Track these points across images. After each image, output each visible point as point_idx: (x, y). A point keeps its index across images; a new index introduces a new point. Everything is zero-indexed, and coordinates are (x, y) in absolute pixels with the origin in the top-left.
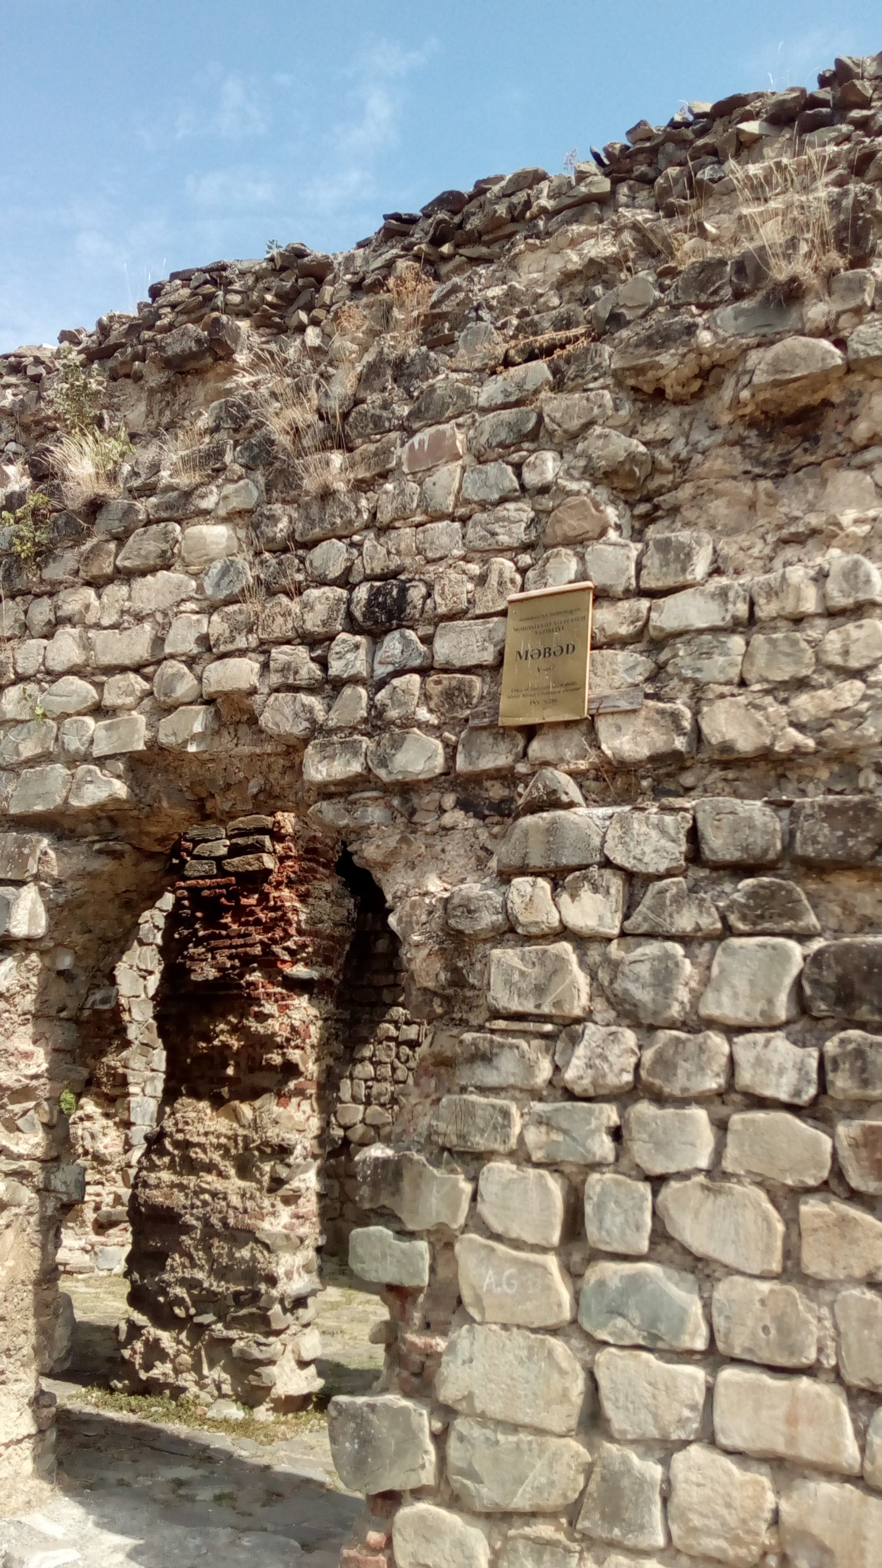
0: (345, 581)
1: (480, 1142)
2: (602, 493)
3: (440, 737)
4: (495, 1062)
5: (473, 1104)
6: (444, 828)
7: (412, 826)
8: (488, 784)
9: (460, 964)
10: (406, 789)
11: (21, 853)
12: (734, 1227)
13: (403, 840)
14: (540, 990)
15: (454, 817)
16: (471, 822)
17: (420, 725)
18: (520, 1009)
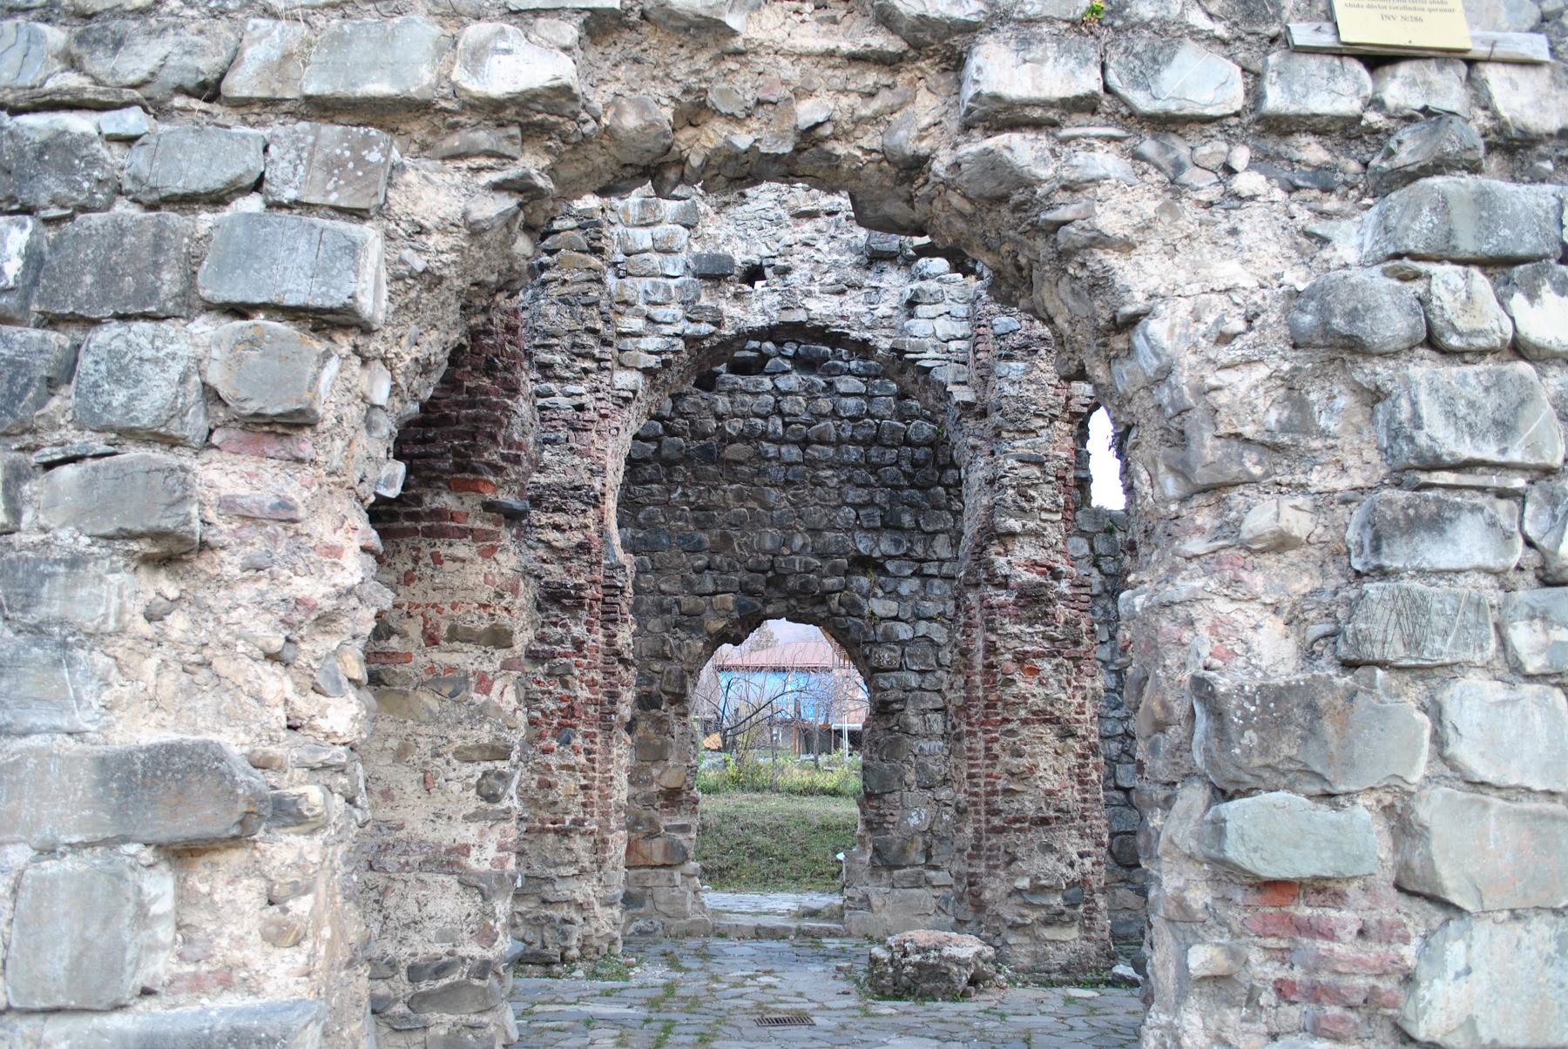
1: (1440, 649)
3: (1231, 57)
4: (1450, 534)
5: (1421, 594)
6: (1237, 196)
7: (1175, 187)
8: (1304, 139)
9: (1313, 397)
11: (360, 162)
13: (1166, 208)
14: (1504, 428)
15: (1247, 181)
16: (1279, 195)
17: (1195, 34)
18: (1477, 455)
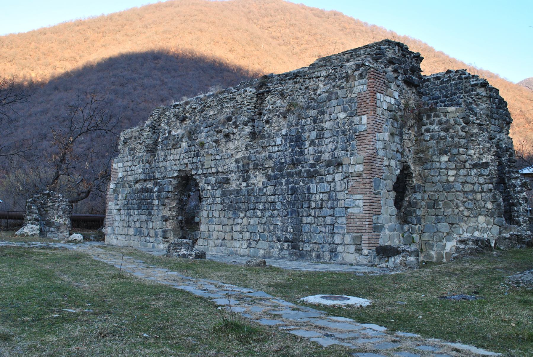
0: (195, 151)
2: (213, 143)
10: (199, 175)
12: (216, 214)
